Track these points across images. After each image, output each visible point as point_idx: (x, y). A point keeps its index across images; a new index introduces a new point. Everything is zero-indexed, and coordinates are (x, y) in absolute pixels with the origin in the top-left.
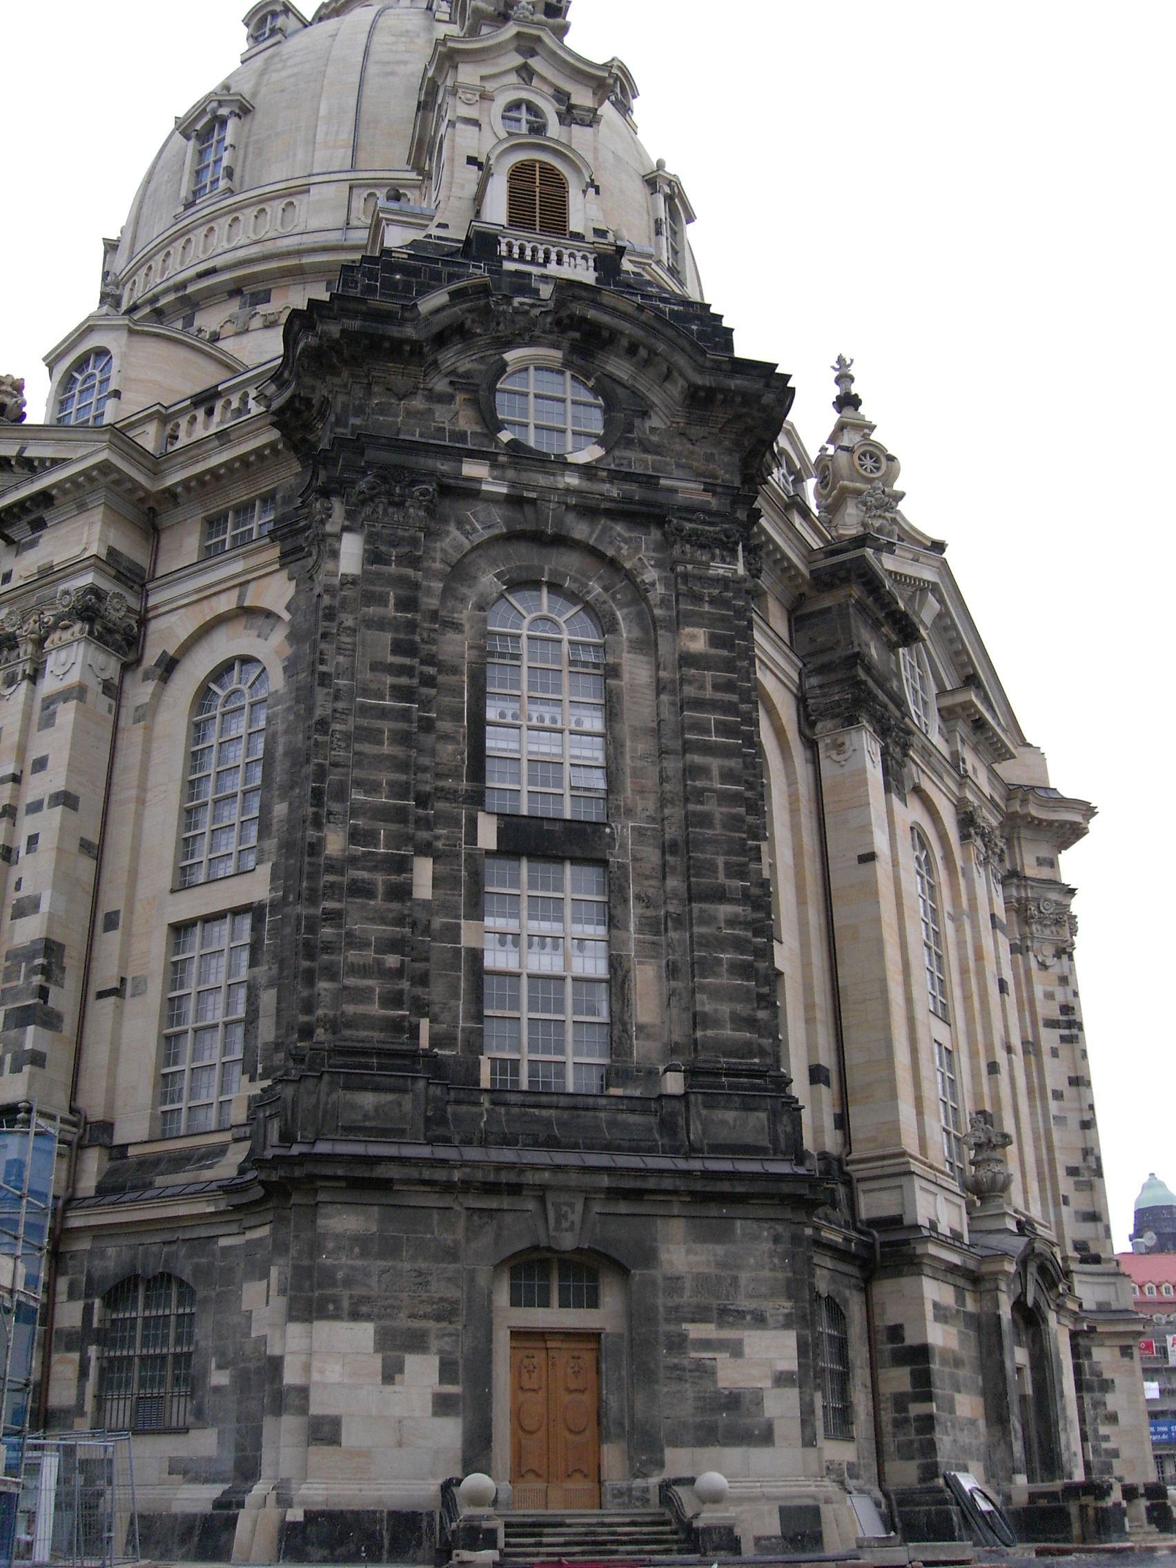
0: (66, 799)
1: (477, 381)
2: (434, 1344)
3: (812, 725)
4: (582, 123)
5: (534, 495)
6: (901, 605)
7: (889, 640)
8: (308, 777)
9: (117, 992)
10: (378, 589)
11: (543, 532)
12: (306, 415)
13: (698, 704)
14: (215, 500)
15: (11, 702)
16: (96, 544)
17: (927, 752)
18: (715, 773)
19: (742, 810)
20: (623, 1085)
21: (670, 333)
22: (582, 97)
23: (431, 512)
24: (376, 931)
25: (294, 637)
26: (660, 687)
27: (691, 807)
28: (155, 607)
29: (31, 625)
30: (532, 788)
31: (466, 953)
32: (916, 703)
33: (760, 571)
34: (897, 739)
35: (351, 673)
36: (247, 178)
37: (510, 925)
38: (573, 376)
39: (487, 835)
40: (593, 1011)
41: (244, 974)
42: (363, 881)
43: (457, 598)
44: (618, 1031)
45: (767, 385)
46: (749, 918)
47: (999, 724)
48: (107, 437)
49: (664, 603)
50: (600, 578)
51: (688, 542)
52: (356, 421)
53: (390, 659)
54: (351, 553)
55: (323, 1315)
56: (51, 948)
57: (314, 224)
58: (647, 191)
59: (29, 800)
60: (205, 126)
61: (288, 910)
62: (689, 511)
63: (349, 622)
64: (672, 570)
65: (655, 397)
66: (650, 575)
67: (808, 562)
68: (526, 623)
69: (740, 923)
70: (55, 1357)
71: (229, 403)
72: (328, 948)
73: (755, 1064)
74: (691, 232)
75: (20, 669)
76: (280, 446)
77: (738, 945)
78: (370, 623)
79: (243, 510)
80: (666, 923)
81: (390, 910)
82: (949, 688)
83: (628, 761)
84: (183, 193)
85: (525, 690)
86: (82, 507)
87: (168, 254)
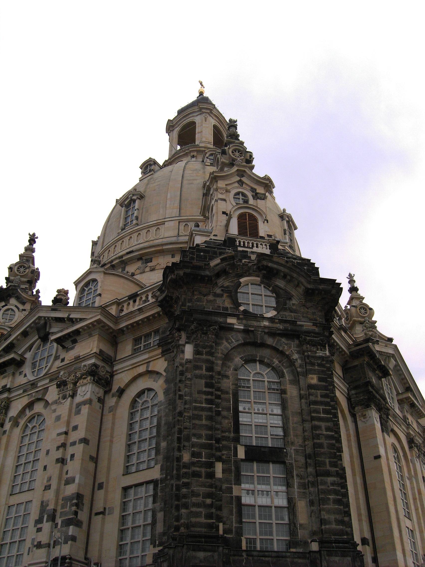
0: (85, 441)
1: (231, 289)
3: (353, 408)
4: (261, 199)
5: (253, 329)
6: (383, 363)
7: (379, 376)
8: (173, 431)
9: (103, 513)
10: (199, 364)
11: (257, 342)
13: (316, 403)
14: (138, 332)
15: (64, 405)
16: (95, 348)
17: (395, 416)
18: (323, 428)
19: (334, 442)
20: (295, 548)
21: (298, 270)
22: (260, 190)
23: (217, 336)
24: (203, 490)
25: (167, 381)
26: (301, 397)
27: (315, 441)
28: (116, 371)
29: (72, 377)
30: (257, 436)
31: (235, 498)
32: (389, 399)
33: (334, 353)
34: (385, 412)
35: (191, 394)
36: (143, 220)
37: (251, 487)
38: (264, 287)
39: (241, 454)
40: (283, 519)
41: (150, 506)
42: (197, 471)
43: (227, 367)
44: (293, 527)
45: (333, 287)
46: (339, 482)
47: (420, 405)
48: (100, 311)
49: (301, 366)
50: (277, 358)
51: (308, 344)
52: (188, 304)
53: (204, 389)
54: (189, 351)
56: (79, 496)
57: (166, 235)
58: (281, 220)
59: (71, 441)
60: (128, 202)
61: (168, 482)
62: (308, 333)
63: (189, 376)
64: (303, 354)
65: (293, 292)
67: (349, 349)
68: (252, 375)
69: (336, 484)
71: (141, 298)
72: (185, 496)
73: (345, 538)
74: (296, 233)
75: (68, 393)
76: (161, 313)
77: (336, 492)
78: (197, 377)
79: (148, 336)
80: (308, 485)
81: (208, 482)
82: (400, 392)
83: (291, 424)
84: (121, 225)
85: (252, 400)
86: (90, 335)
87: (116, 246)
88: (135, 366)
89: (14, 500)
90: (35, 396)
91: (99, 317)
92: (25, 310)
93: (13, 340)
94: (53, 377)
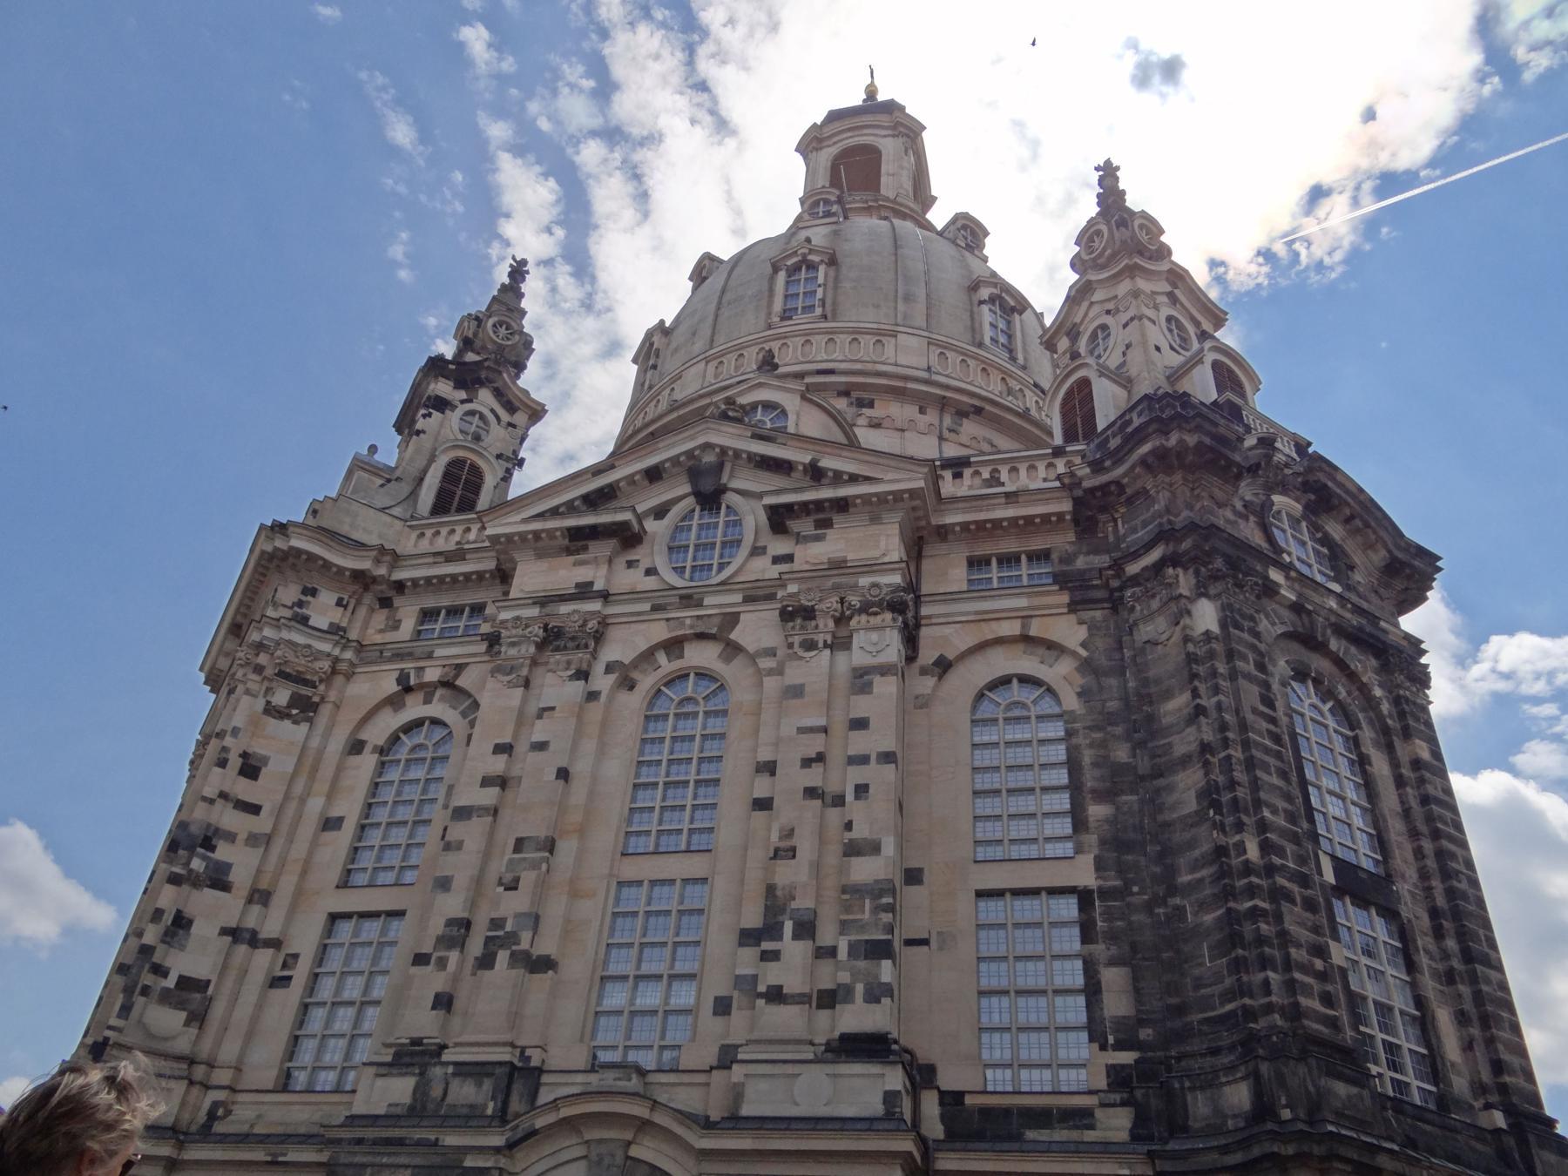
0: (888, 757)
12: (1112, 498)
14: (993, 547)
26: (1400, 782)
28: (930, 617)
48: (926, 470)
54: (1206, 616)
65: (1357, 558)
66: (1378, 692)
75: (820, 638)
76: (1068, 517)
84: (778, 305)
86: (875, 520)
88: (984, 618)
90: (692, 627)
91: (922, 484)
92: (514, 426)
93: (618, 481)
94: (756, 595)
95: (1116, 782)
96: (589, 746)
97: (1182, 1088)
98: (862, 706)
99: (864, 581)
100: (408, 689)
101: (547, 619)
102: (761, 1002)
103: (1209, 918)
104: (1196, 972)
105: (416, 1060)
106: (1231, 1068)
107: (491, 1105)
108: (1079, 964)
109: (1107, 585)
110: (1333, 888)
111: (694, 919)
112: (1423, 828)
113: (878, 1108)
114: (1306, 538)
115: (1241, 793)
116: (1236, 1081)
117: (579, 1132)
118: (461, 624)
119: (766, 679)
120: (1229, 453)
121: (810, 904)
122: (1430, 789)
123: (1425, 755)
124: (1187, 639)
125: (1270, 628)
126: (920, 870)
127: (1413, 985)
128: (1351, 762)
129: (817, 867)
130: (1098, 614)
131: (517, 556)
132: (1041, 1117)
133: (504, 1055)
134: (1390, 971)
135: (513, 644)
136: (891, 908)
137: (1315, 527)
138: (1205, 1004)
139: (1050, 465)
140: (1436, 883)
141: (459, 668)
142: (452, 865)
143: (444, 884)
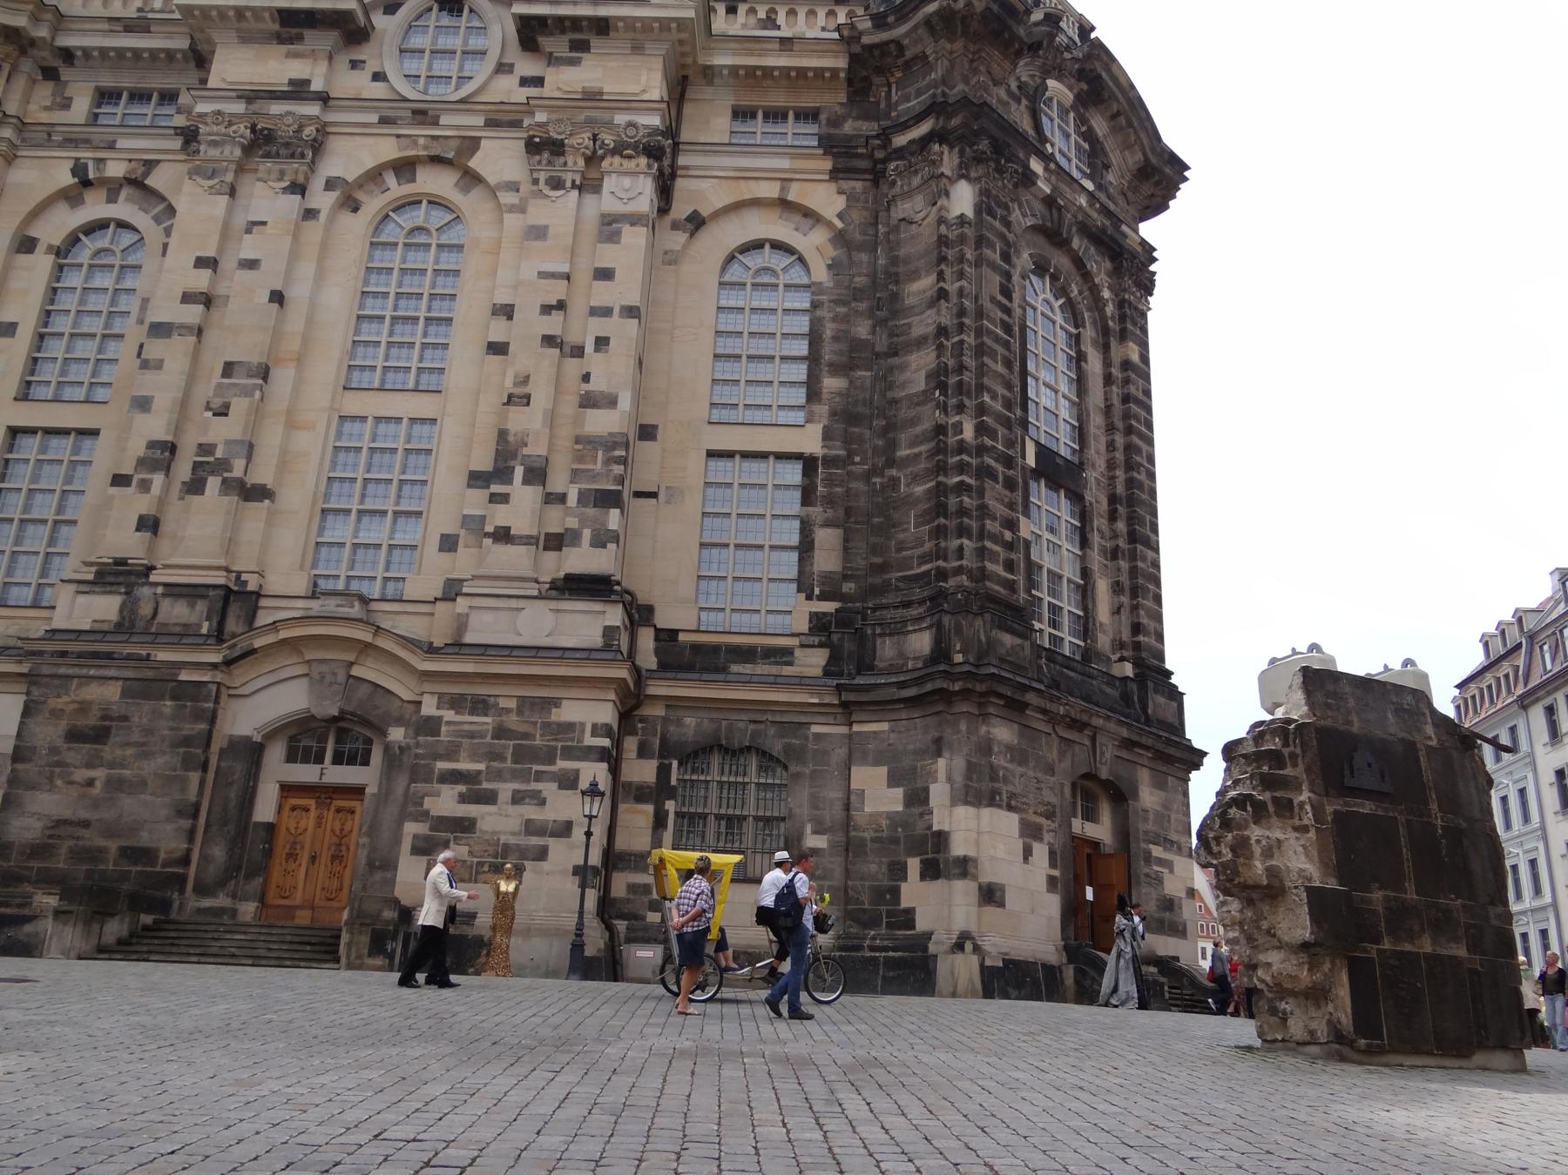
0: (631, 312)
2: (1048, 837)
12: (889, 60)
14: (762, 97)
26: (1108, 380)
28: (686, 168)
44: (1086, 626)
49: (1113, 318)
54: (963, 199)
55: (992, 803)
65: (1115, 158)
66: (1106, 294)
70: (622, 807)
75: (568, 178)
79: (775, 115)
86: (637, 49)
88: (744, 176)
89: (353, 404)
90: (426, 148)
91: (691, 14)
94: (501, 120)
95: (854, 357)
96: (307, 269)
97: (874, 634)
98: (608, 256)
99: (621, 119)
100: (86, 183)
101: (255, 119)
102: (488, 542)
103: (919, 490)
104: (901, 536)
105: (121, 579)
106: (920, 619)
107: (206, 625)
108: (796, 524)
109: (871, 156)
110: (1033, 470)
111: (422, 457)
112: (1119, 424)
113: (598, 641)
114: (1071, 130)
115: (967, 377)
116: (920, 630)
117: (301, 653)
118: (149, 109)
119: (506, 216)
120: (1014, 27)
121: (542, 451)
122: (1132, 389)
123: (1135, 358)
124: (941, 221)
125: (1021, 219)
126: (655, 427)
127: (1083, 558)
128: (1070, 358)
129: (552, 418)
130: (859, 185)
131: (216, 35)
132: (746, 654)
133: (219, 579)
134: (1066, 545)
135: (214, 144)
136: (623, 461)
137: (1082, 120)
138: (905, 564)
139: (831, 13)
140: (1120, 474)
141: (150, 165)
142: (148, 383)
143: (143, 404)
